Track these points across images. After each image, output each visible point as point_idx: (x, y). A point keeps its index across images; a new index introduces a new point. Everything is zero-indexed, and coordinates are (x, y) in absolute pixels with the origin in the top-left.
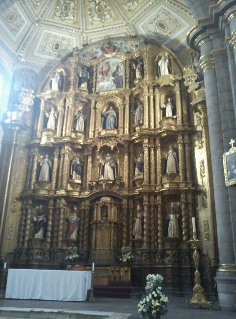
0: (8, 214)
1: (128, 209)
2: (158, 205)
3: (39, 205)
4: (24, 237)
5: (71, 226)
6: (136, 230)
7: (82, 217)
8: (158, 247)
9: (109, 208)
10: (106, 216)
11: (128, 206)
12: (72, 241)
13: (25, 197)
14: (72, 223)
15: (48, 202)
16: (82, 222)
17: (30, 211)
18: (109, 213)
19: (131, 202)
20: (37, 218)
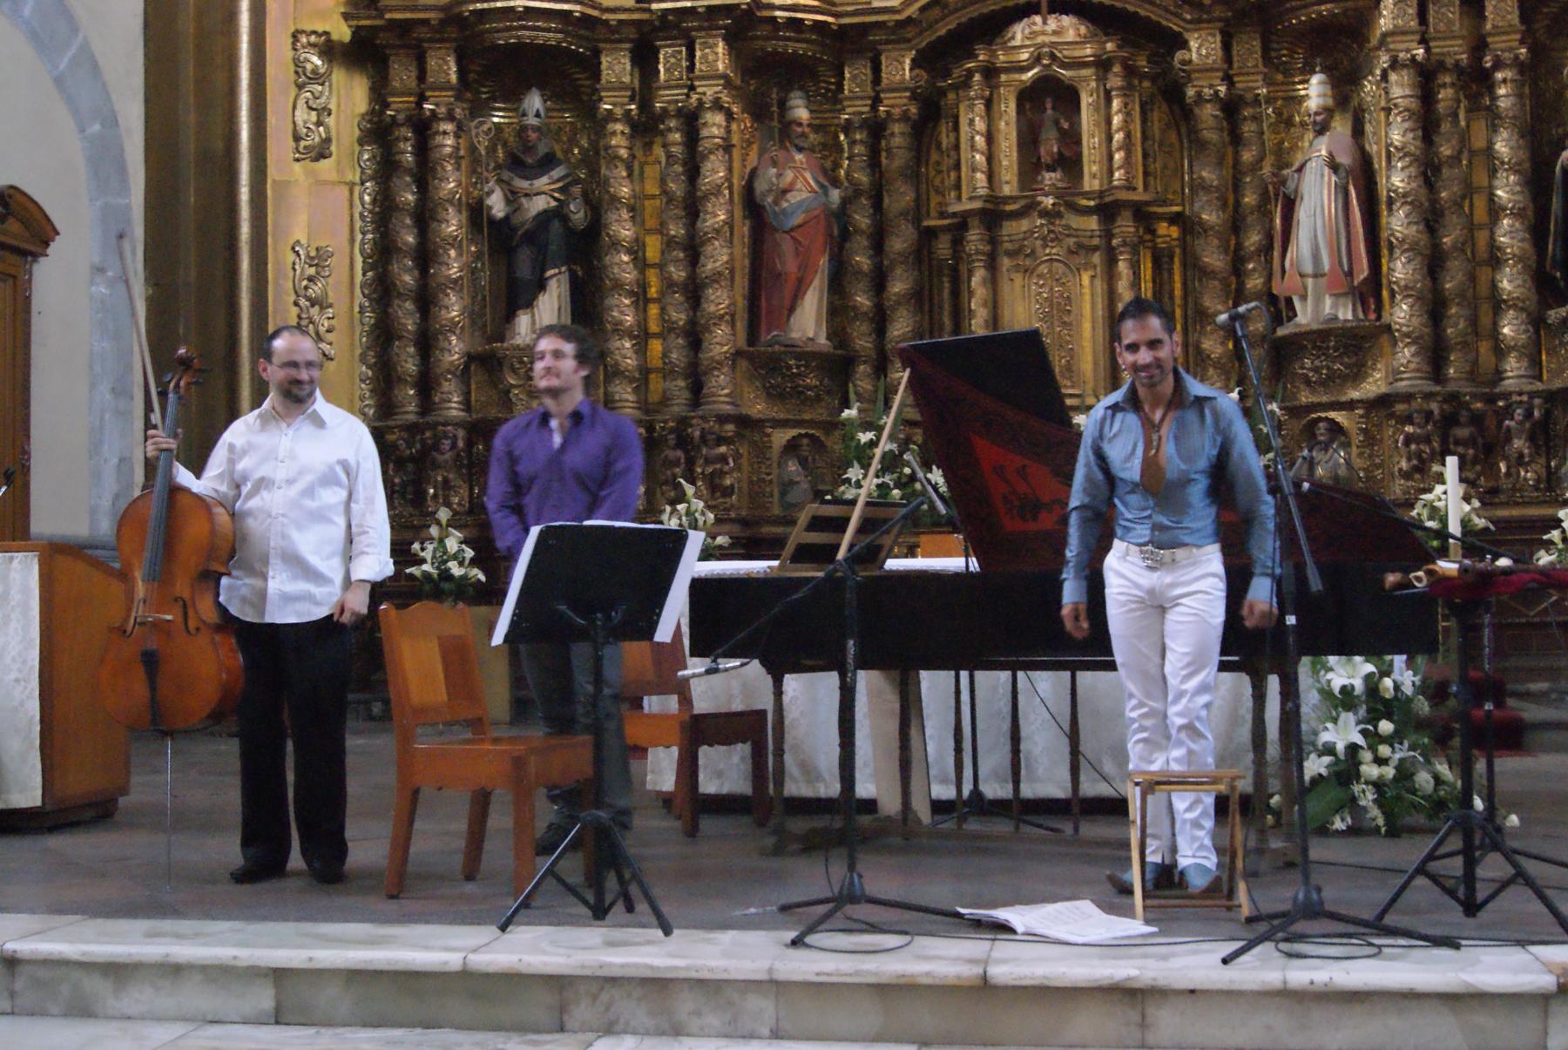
0: (273, 173)
1: (1231, 108)
2: (1498, 65)
3: (512, 96)
4: (427, 343)
5: (787, 245)
6: (1308, 268)
7: (862, 177)
8: (1499, 375)
9: (1086, 100)
10: (1070, 163)
11: (1228, 79)
12: (807, 357)
13: (404, 27)
14: (797, 220)
15: (592, 68)
16: (862, 219)
17: (450, 141)
18: (1091, 142)
19: (1249, 49)
20: (512, 197)
